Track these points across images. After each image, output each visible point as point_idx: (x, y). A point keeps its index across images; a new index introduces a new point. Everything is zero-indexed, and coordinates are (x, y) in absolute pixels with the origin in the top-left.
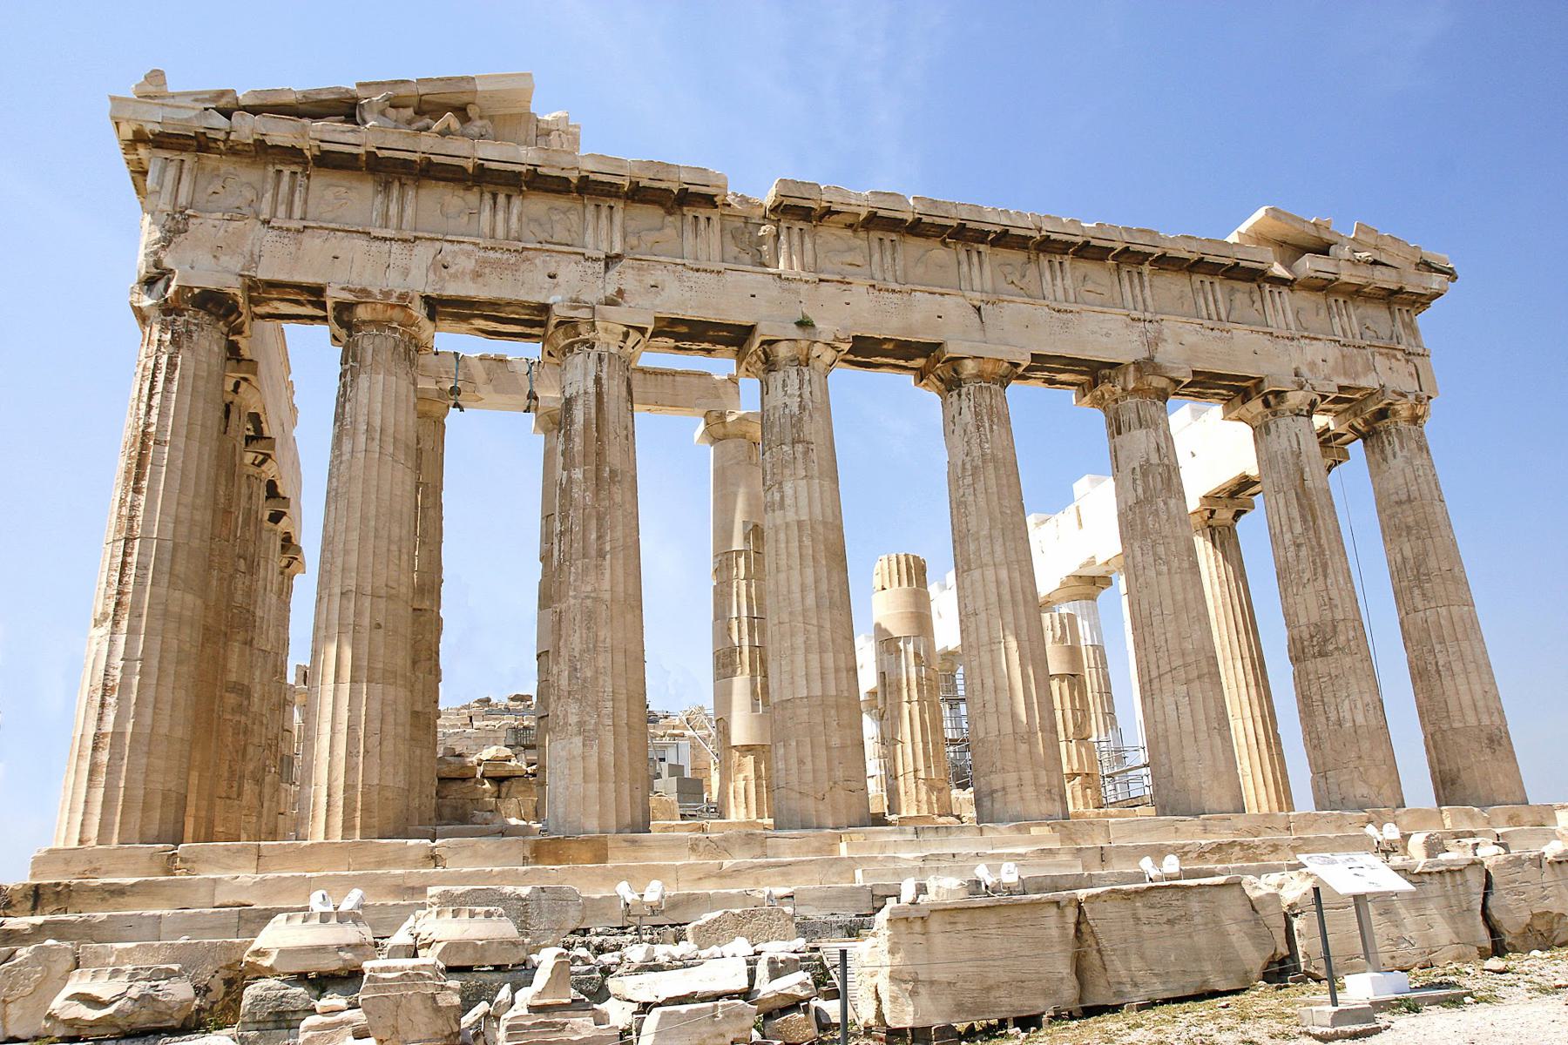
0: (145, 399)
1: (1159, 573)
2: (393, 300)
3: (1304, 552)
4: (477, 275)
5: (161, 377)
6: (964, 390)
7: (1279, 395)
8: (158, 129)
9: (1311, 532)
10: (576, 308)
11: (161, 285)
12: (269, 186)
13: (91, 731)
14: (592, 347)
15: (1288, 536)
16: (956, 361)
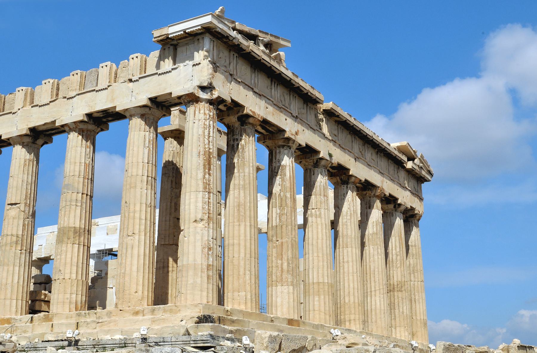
0: (207, 137)
1: (378, 258)
2: (260, 119)
3: (399, 258)
4: (273, 115)
5: (211, 130)
6: (349, 186)
7: (400, 205)
8: (220, 31)
9: (401, 252)
10: (292, 135)
11: (208, 90)
12: (232, 60)
13: (205, 264)
14: (290, 149)
15: (394, 251)
16: (352, 176)
